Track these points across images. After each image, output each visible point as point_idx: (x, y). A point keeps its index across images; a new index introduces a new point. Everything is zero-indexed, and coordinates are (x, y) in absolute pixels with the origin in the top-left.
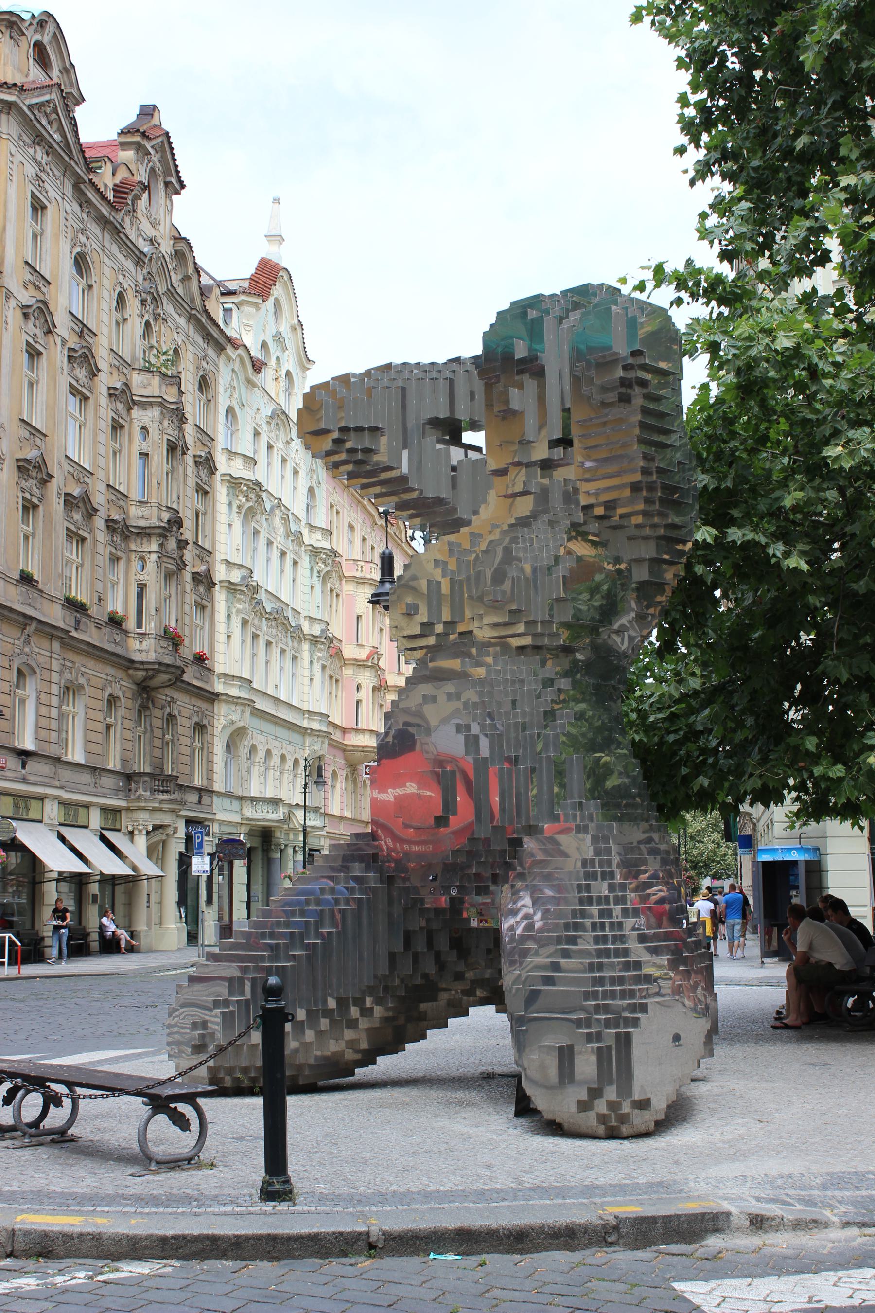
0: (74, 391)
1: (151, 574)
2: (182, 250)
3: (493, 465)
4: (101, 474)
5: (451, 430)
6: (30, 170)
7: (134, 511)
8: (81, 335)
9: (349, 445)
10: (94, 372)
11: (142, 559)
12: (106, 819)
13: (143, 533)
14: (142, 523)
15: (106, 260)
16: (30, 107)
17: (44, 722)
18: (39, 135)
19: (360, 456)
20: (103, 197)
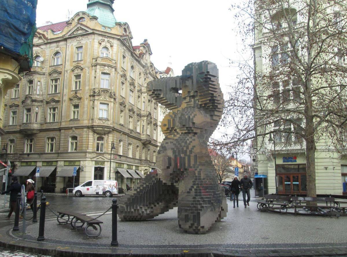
0: (131, 90)
1: (145, 123)
2: (152, 65)
3: (183, 97)
4: (136, 105)
5: (176, 90)
6: (123, 51)
7: (142, 112)
8: (132, 80)
9: (155, 93)
10: (135, 87)
11: (143, 121)
12: (136, 168)
13: (144, 116)
14: (143, 114)
15: (137, 67)
16: (123, 39)
17: (124, 150)
18: (124, 44)
19: (158, 95)
20: (137, 56)
